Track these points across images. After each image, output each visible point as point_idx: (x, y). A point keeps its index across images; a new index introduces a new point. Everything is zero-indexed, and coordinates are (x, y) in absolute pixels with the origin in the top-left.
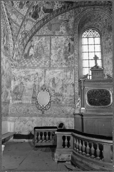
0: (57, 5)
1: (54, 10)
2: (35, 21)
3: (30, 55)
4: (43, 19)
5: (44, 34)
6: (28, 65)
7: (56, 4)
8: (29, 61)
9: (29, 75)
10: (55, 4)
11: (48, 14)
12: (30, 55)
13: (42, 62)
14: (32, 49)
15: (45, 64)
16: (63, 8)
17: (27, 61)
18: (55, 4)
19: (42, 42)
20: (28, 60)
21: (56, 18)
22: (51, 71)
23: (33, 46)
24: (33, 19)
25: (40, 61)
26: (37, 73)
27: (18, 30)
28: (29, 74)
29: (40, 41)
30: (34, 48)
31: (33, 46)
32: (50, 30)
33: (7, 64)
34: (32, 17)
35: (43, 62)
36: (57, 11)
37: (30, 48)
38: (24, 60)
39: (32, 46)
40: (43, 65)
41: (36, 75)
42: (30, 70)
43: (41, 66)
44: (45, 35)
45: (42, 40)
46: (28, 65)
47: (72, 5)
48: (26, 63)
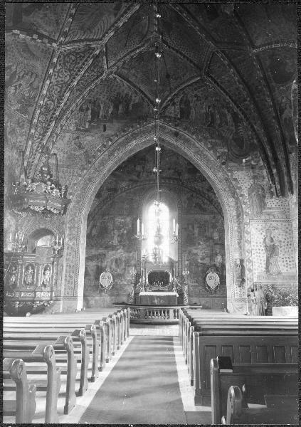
4: (107, 198)
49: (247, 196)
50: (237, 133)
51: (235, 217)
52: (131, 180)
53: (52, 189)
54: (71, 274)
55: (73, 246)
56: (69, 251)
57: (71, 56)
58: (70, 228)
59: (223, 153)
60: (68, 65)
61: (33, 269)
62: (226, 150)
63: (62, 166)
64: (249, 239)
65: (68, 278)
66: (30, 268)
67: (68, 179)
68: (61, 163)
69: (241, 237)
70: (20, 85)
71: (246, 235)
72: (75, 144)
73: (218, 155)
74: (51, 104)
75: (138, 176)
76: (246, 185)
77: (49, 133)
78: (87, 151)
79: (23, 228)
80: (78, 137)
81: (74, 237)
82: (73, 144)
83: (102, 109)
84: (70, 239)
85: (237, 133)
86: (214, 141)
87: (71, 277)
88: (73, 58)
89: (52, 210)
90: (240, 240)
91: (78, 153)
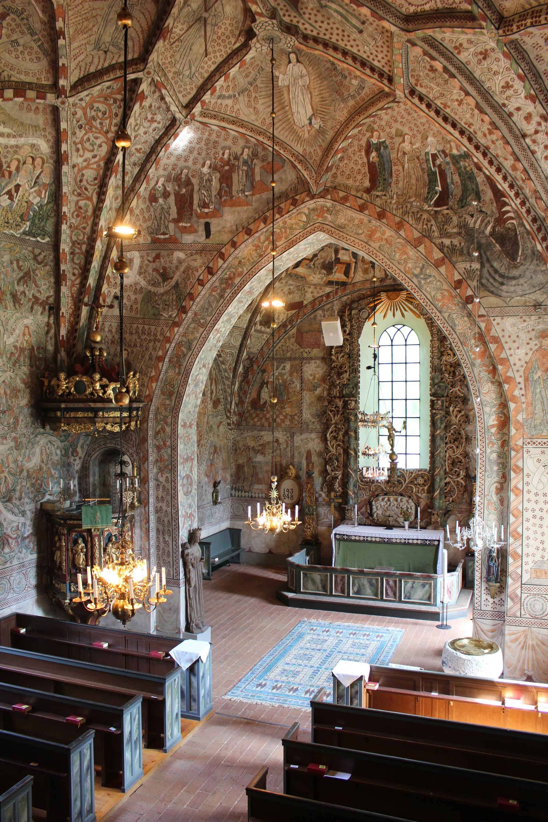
0: (312, 292)
1: (305, 303)
2: (268, 330)
3: (262, 402)
5: (289, 355)
6: (258, 423)
7: (310, 290)
8: (261, 415)
9: (262, 445)
10: (306, 292)
11: (294, 311)
12: (262, 402)
13: (285, 417)
14: (265, 389)
15: (291, 421)
16: (324, 298)
17: (257, 416)
18: (306, 292)
19: (285, 374)
20: (258, 412)
21: (312, 316)
22: (304, 436)
23: (267, 383)
24: (263, 329)
25: (281, 413)
26: (277, 441)
27: (235, 355)
28: (261, 442)
29: (279, 370)
30: (269, 386)
31: (267, 383)
32: (301, 346)
33: (221, 428)
34: (261, 324)
35: (289, 417)
36: (313, 302)
37: (261, 387)
38: (252, 412)
39: (264, 383)
40: (287, 422)
41: (276, 444)
42: (262, 433)
43: (283, 425)
44: (290, 359)
45: (284, 368)
46: (258, 423)
47: (345, 289)
48: (256, 420)
49: (521, 380)
50: (500, 220)
51: (493, 430)
52: (330, 283)
53: (104, 387)
54: (167, 539)
55: (166, 485)
56: (160, 493)
57: (96, 105)
58: (159, 448)
59: (469, 273)
60: (97, 124)
61: (85, 542)
62: (476, 266)
63: (134, 320)
64: (520, 486)
65: (162, 545)
66: (80, 541)
67: (147, 349)
68: (133, 314)
69: (504, 479)
70: (18, 187)
71: (513, 475)
72: (155, 270)
73: (457, 277)
74: (86, 205)
75: (347, 273)
76: (521, 353)
77: (95, 264)
78: (177, 284)
79: (79, 449)
80: (158, 257)
81: (166, 467)
82: (151, 271)
83: (196, 188)
84: (161, 470)
85: (500, 220)
86: (447, 242)
87: (165, 542)
88: (102, 107)
89: (109, 427)
90: (501, 484)
91: (161, 290)
